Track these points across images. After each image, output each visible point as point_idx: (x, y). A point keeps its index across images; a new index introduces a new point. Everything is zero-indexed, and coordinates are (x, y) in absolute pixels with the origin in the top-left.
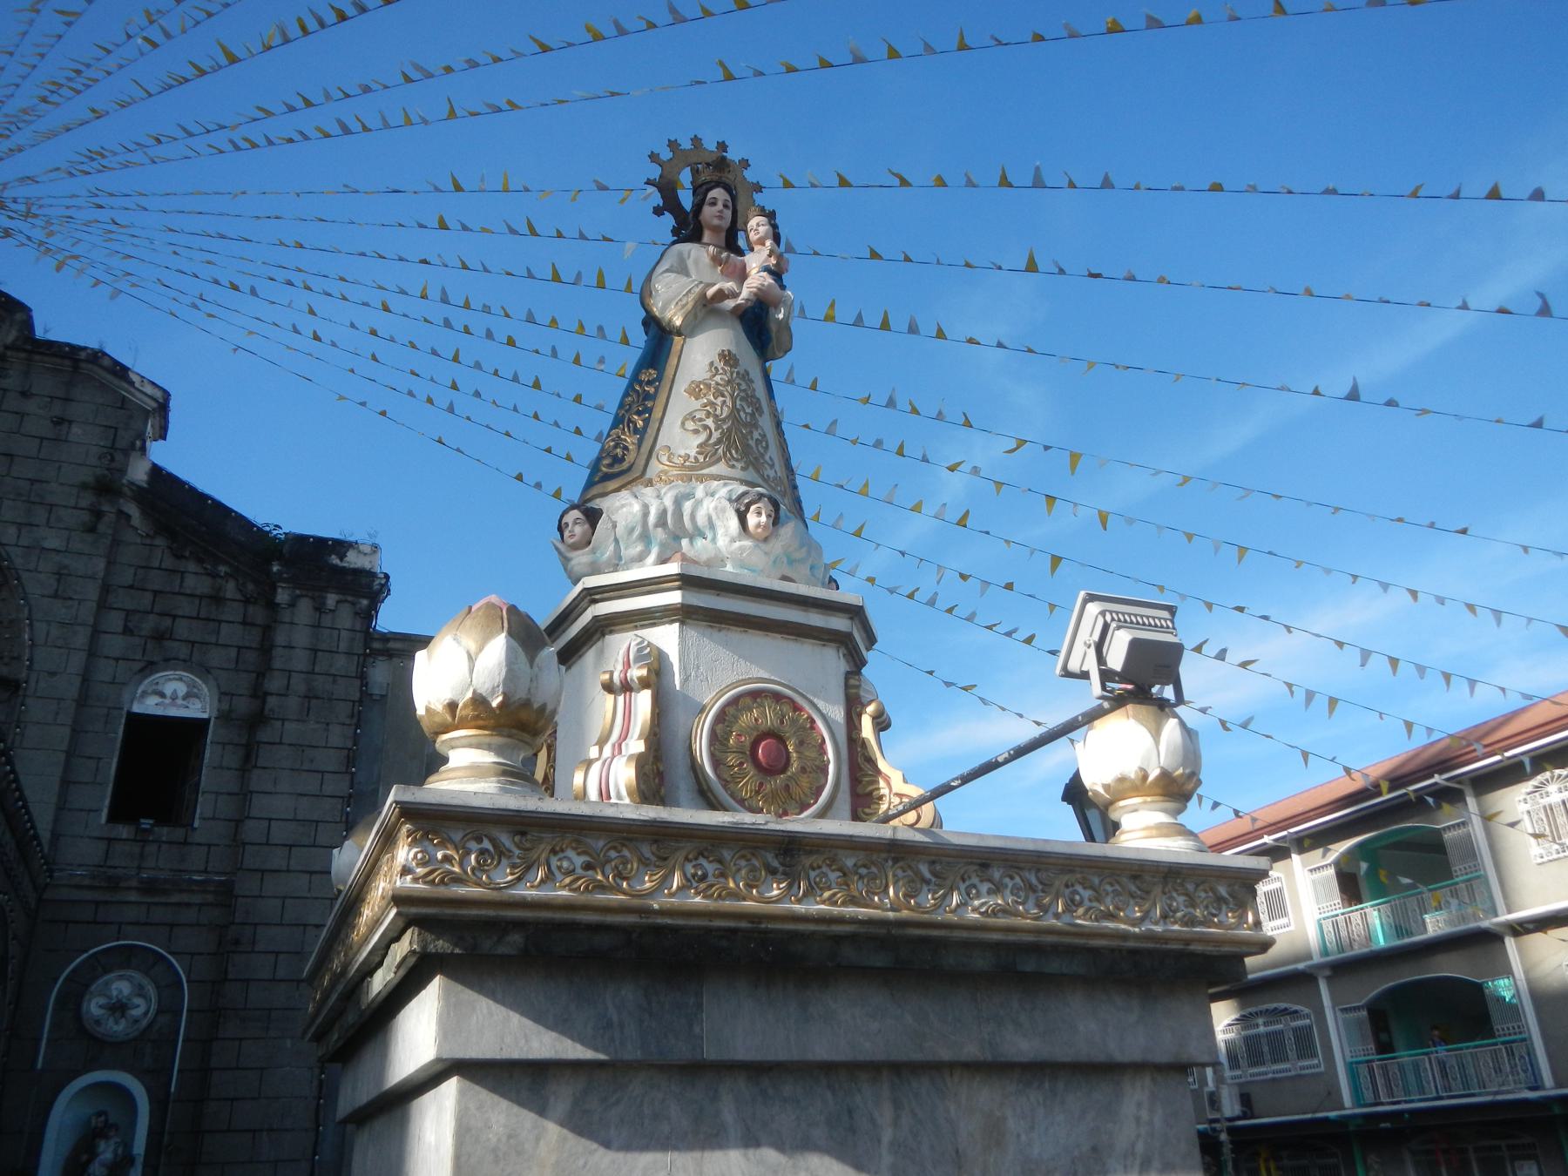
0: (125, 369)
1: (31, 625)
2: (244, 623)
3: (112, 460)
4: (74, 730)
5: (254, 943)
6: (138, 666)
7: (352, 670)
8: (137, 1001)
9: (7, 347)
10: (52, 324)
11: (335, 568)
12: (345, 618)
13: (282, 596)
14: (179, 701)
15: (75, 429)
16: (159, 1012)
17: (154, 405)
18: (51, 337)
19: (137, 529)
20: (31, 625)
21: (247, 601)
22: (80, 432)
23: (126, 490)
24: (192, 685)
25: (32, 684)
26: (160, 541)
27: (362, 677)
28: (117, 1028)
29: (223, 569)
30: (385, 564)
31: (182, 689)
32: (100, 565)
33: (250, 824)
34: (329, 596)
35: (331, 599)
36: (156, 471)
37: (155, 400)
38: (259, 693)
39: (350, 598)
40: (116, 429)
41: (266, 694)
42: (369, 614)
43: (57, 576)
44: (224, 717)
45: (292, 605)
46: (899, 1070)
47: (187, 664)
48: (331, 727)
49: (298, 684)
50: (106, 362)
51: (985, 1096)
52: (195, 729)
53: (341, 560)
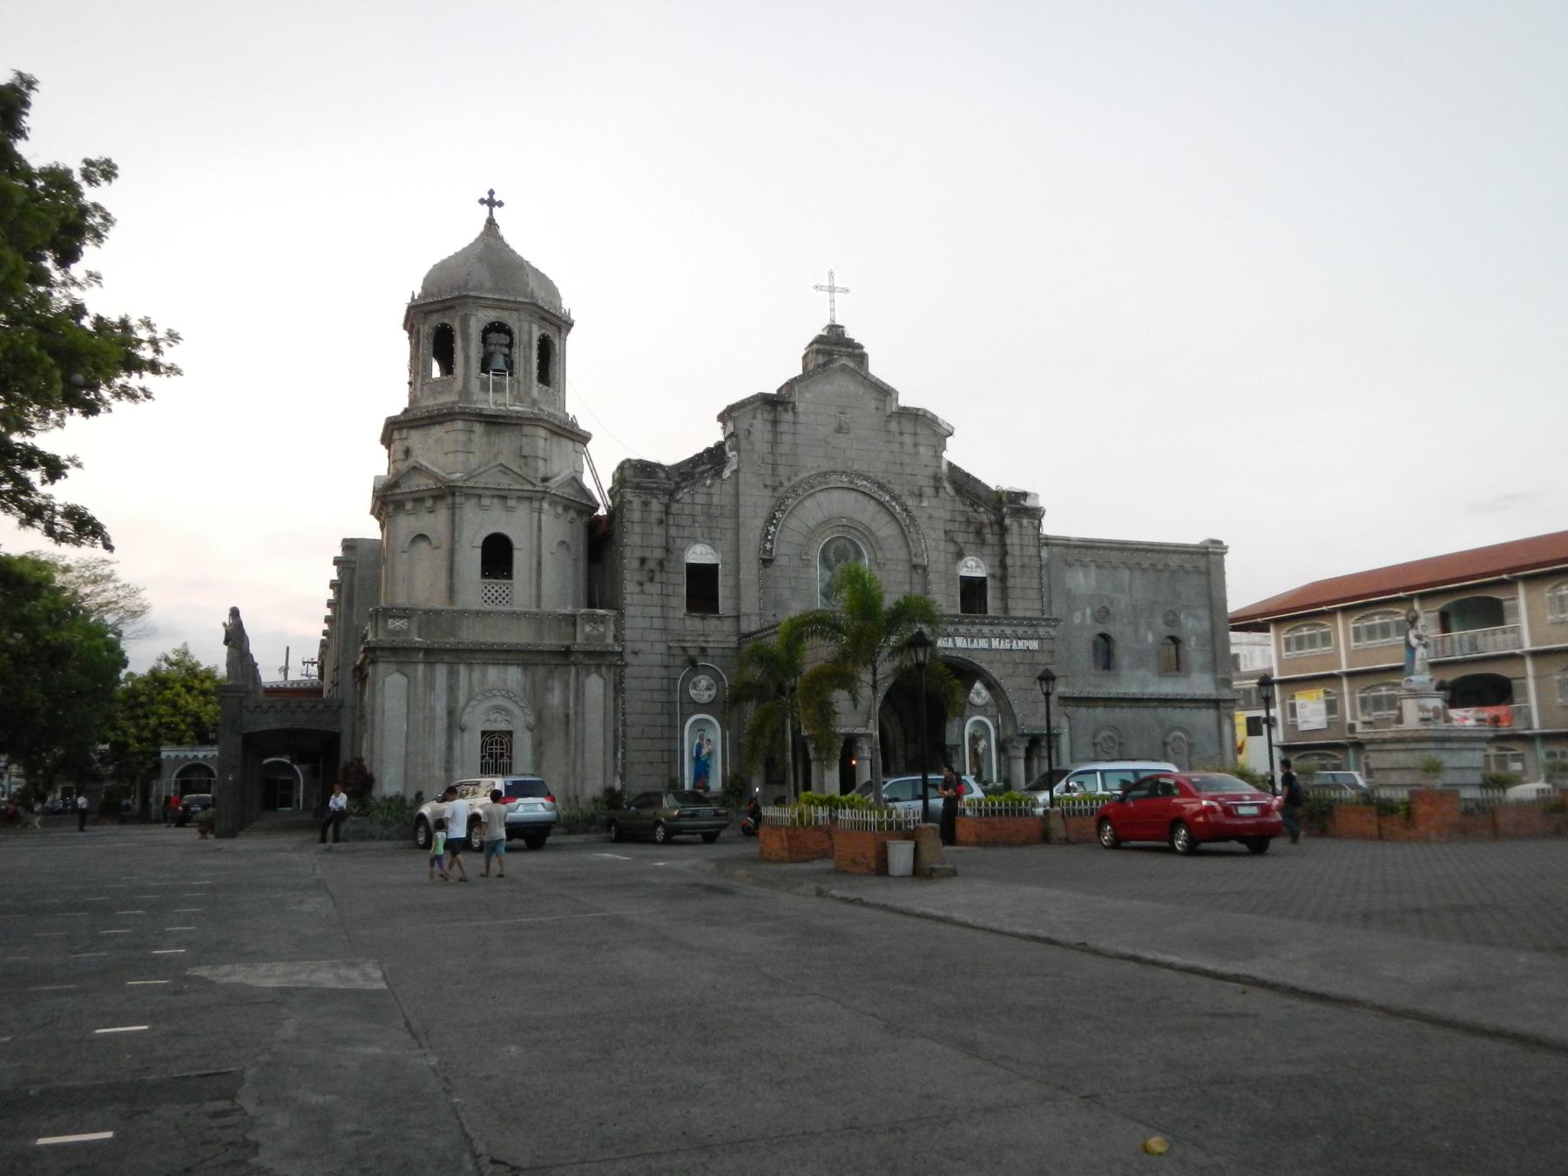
0: (937, 418)
12: (1030, 531)
13: (1007, 521)
15: (922, 450)
18: (909, 404)
23: (944, 477)
24: (976, 562)
26: (957, 498)
30: (1042, 502)
31: (974, 564)
35: (1025, 522)
36: (950, 464)
44: (993, 576)
49: (1018, 563)
50: (929, 416)
52: (983, 581)
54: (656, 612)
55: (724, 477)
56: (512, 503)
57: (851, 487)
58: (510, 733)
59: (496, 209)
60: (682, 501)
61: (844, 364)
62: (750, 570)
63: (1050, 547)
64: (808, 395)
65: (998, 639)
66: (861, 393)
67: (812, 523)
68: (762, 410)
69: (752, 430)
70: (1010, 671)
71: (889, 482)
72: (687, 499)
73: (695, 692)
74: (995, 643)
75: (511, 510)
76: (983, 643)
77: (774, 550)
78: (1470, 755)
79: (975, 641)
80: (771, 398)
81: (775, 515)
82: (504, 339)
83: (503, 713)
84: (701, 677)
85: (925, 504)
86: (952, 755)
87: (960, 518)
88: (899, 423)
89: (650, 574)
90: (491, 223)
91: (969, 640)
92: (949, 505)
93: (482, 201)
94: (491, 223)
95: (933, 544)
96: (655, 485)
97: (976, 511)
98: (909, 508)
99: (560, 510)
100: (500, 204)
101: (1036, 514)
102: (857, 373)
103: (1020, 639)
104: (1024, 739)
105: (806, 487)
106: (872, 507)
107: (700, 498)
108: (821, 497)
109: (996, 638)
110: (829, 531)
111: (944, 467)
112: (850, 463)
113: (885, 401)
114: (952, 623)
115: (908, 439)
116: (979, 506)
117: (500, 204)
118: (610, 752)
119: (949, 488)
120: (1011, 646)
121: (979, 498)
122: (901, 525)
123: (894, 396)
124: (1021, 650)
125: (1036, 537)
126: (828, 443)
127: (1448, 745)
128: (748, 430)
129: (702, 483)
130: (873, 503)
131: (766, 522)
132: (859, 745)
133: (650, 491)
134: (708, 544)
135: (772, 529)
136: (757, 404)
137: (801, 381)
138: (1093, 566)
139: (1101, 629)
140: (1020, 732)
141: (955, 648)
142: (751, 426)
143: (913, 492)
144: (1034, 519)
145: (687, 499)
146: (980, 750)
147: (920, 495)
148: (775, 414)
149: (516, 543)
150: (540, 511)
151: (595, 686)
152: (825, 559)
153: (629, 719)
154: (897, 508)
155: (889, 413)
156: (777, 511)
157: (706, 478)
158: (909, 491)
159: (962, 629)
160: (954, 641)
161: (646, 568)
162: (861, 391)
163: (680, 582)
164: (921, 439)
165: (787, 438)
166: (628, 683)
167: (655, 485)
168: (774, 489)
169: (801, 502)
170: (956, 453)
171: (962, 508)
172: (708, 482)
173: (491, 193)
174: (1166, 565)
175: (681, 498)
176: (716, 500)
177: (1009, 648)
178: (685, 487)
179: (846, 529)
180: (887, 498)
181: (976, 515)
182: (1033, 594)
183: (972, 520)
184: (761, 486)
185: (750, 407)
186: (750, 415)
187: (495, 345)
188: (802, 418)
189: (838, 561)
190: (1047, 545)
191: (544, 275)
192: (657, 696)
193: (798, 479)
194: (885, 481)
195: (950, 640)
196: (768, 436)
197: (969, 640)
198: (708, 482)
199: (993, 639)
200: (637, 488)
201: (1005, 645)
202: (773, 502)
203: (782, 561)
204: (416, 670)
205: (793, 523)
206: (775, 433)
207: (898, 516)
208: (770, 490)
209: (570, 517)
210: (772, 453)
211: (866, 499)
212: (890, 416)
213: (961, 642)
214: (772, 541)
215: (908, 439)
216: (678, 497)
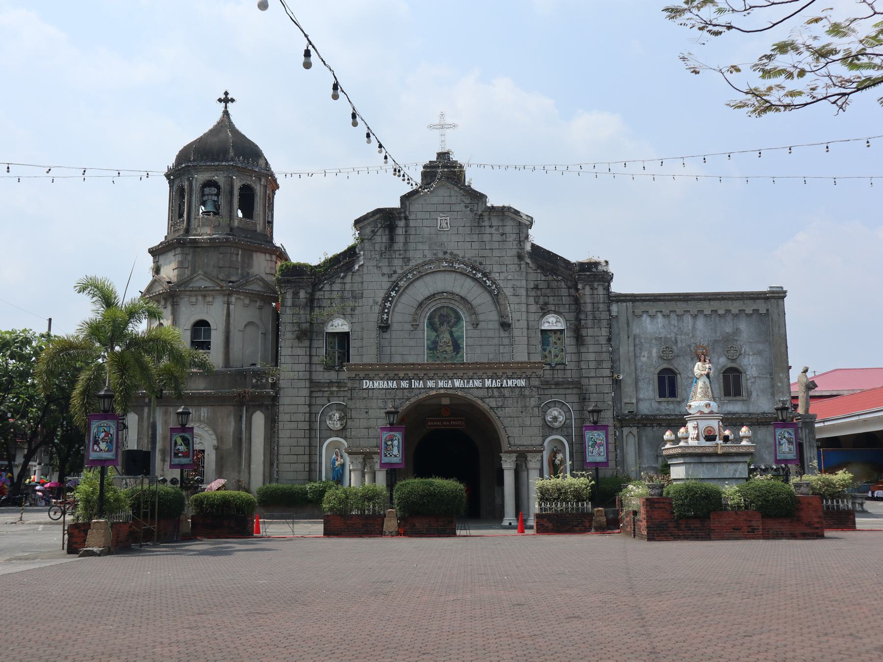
0: (519, 212)
1: (509, 306)
2: (569, 296)
3: (521, 245)
4: (528, 337)
5: (589, 399)
6: (541, 314)
8: (560, 416)
10: (494, 200)
12: (601, 291)
13: (580, 286)
14: (554, 324)
16: (566, 419)
20: (509, 306)
21: (569, 288)
25: (513, 324)
26: (539, 271)
27: (609, 311)
28: (557, 424)
29: (560, 278)
30: (611, 269)
31: (554, 320)
32: (524, 283)
33: (582, 363)
36: (533, 245)
38: (578, 320)
39: (601, 283)
41: (581, 320)
42: (607, 288)
45: (584, 288)
46: (719, 462)
47: (555, 312)
51: (727, 464)
54: (302, 367)
56: (210, 299)
58: (203, 451)
59: (229, 104)
60: (324, 289)
62: (371, 335)
63: (619, 303)
65: (490, 380)
67: (420, 298)
70: (500, 404)
71: (481, 264)
73: (330, 422)
74: (488, 383)
75: (210, 304)
76: (477, 383)
77: (390, 320)
78: (732, 467)
79: (471, 381)
82: (214, 190)
83: (199, 438)
84: (334, 412)
86: (522, 466)
88: (489, 219)
90: (226, 113)
91: (466, 381)
92: (532, 276)
93: (220, 100)
94: (226, 113)
95: (516, 307)
99: (247, 301)
100: (232, 100)
101: (606, 278)
103: (509, 378)
105: (415, 273)
106: (469, 283)
107: (337, 287)
108: (428, 279)
109: (488, 379)
110: (434, 303)
111: (528, 248)
114: (452, 369)
117: (232, 100)
118: (268, 465)
120: (502, 385)
127: (705, 460)
130: (469, 280)
131: (383, 300)
134: (342, 318)
135: (388, 304)
136: (378, 216)
138: (659, 315)
139: (665, 366)
141: (454, 388)
144: (604, 282)
145: (327, 287)
146: (557, 462)
149: (213, 326)
150: (229, 304)
151: (259, 419)
152: (431, 324)
153: (281, 442)
154: (487, 282)
159: (460, 374)
160: (453, 383)
163: (321, 346)
166: (282, 417)
168: (390, 276)
169: (411, 283)
170: (538, 237)
172: (342, 274)
173: (226, 93)
174: (728, 311)
175: (322, 288)
176: (348, 287)
178: (326, 279)
179: (447, 301)
182: (603, 340)
184: (380, 275)
185: (372, 219)
187: (208, 195)
188: (412, 223)
189: (442, 324)
190: (617, 301)
191: (256, 145)
192: (301, 425)
193: (408, 267)
195: (450, 382)
197: (466, 381)
198: (342, 274)
199: (486, 380)
201: (496, 383)
202: (389, 284)
203: (395, 326)
204: (143, 411)
205: (405, 299)
208: (387, 276)
209: (258, 304)
213: (458, 383)
214: (388, 313)
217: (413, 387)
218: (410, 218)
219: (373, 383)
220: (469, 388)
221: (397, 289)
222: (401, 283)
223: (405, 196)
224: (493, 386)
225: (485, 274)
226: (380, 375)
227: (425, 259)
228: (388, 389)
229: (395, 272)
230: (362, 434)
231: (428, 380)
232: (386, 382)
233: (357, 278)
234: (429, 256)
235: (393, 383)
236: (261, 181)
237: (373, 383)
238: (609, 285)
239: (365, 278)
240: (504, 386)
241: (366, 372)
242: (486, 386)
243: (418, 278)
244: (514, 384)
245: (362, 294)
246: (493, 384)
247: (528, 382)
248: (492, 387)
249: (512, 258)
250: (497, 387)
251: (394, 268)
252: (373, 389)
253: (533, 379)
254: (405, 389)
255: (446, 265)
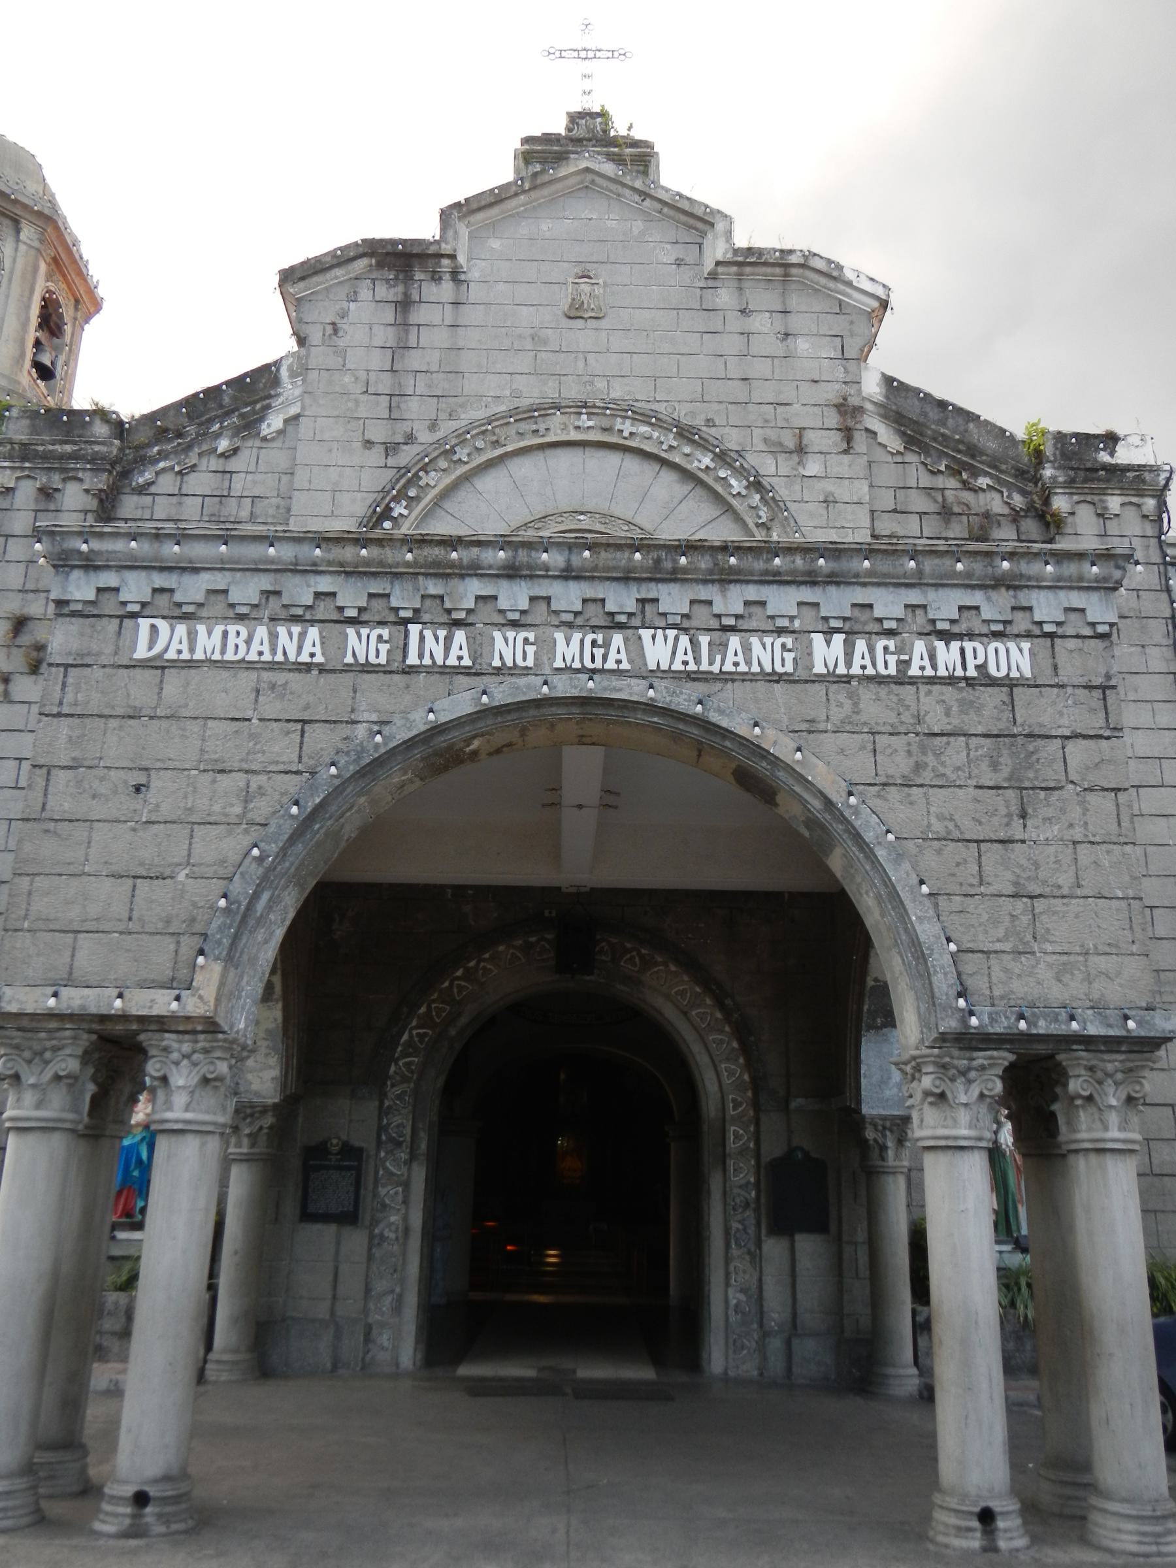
0: (840, 267)
7: (1154, 581)
9: (718, 263)
11: (1107, 468)
13: (1060, 503)
15: (803, 346)
17: (875, 304)
19: (885, 447)
22: (806, 346)
23: (869, 406)
26: (911, 457)
34: (1109, 498)
35: (1114, 503)
37: (877, 298)
39: (1134, 500)
40: (842, 337)
43: (825, 505)
48: (1147, 650)
53: (1112, 454)
55: (265, 430)
57: (614, 439)
60: (153, 489)
61: (587, 170)
64: (495, 244)
65: (838, 639)
66: (636, 231)
68: (373, 280)
69: (344, 326)
71: (710, 423)
72: (167, 483)
80: (389, 248)
81: (388, 509)
85: (813, 467)
86: (883, 1148)
87: (920, 503)
89: (34, 654)
92: (888, 474)
96: (68, 448)
97: (967, 487)
98: (765, 482)
102: (624, 185)
103: (946, 637)
104: (981, 1058)
105: (480, 444)
107: (200, 482)
108: (523, 468)
109: (829, 633)
111: (872, 387)
112: (601, 384)
113: (700, 245)
114: (627, 578)
115: (761, 323)
116: (975, 473)
119: (886, 435)
121: (973, 451)
122: (745, 525)
123: (720, 226)
124: (951, 680)
125: (1154, 541)
126: (545, 342)
128: (333, 324)
129: (205, 447)
132: (153, 1068)
133: (64, 466)
137: (473, 212)
140: (950, 1024)
142: (344, 315)
143: (780, 444)
144: (1141, 494)
145: (167, 483)
147: (801, 450)
148: (407, 288)
154: (733, 482)
155: (709, 265)
156: (394, 499)
157: (218, 435)
158: (765, 440)
160: (636, 649)
161: (25, 639)
162: (638, 226)
164: (796, 322)
165: (433, 338)
167: (68, 448)
169: (466, 478)
171: (926, 481)
172: (223, 444)
177: (892, 670)
178: (163, 456)
180: (707, 461)
181: (967, 496)
183: (956, 509)
186: (343, 292)
188: (475, 293)
193: (454, 425)
194: (699, 421)
196: (385, 336)
197: (704, 640)
198: (223, 444)
200: (24, 459)
206: (403, 325)
207: (734, 502)
210: (392, 370)
211: (651, 468)
212: (713, 276)
215: (761, 323)
216: (141, 480)
217: (413, 659)
218: (474, 274)
219: (192, 636)
220: (725, 678)
221: (412, 493)
222: (431, 478)
223: (457, 205)
224: (856, 670)
225: (722, 457)
226: (234, 597)
227: (517, 403)
228: (272, 666)
229: (410, 439)
230: (94, 910)
231: (500, 626)
232: (262, 632)
233: (275, 457)
234: (532, 393)
235: (303, 636)
236: (18, 231)
237: (192, 636)
238: (1162, 506)
239: (304, 453)
240: (914, 671)
241: (160, 580)
242: (819, 669)
243: (491, 464)
244: (971, 663)
245: (289, 510)
246: (857, 661)
247: (1047, 664)
248: (847, 679)
249: (817, 410)
250: (879, 680)
251: (405, 427)
252: (190, 664)
253: (1071, 644)
254: (367, 668)
255: (590, 423)
